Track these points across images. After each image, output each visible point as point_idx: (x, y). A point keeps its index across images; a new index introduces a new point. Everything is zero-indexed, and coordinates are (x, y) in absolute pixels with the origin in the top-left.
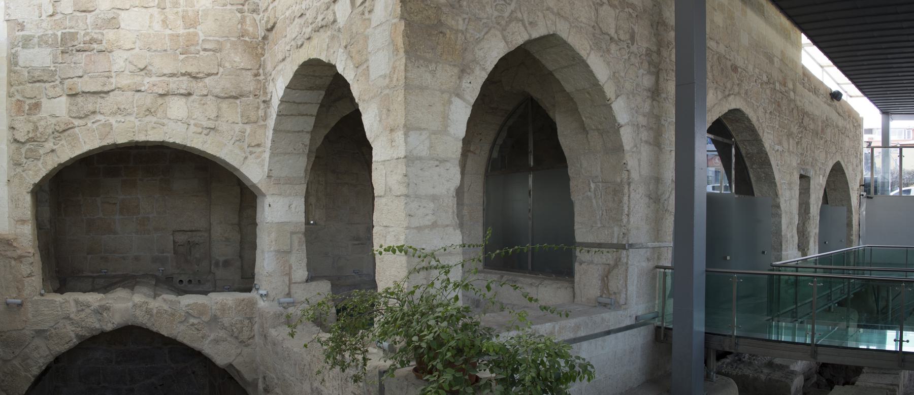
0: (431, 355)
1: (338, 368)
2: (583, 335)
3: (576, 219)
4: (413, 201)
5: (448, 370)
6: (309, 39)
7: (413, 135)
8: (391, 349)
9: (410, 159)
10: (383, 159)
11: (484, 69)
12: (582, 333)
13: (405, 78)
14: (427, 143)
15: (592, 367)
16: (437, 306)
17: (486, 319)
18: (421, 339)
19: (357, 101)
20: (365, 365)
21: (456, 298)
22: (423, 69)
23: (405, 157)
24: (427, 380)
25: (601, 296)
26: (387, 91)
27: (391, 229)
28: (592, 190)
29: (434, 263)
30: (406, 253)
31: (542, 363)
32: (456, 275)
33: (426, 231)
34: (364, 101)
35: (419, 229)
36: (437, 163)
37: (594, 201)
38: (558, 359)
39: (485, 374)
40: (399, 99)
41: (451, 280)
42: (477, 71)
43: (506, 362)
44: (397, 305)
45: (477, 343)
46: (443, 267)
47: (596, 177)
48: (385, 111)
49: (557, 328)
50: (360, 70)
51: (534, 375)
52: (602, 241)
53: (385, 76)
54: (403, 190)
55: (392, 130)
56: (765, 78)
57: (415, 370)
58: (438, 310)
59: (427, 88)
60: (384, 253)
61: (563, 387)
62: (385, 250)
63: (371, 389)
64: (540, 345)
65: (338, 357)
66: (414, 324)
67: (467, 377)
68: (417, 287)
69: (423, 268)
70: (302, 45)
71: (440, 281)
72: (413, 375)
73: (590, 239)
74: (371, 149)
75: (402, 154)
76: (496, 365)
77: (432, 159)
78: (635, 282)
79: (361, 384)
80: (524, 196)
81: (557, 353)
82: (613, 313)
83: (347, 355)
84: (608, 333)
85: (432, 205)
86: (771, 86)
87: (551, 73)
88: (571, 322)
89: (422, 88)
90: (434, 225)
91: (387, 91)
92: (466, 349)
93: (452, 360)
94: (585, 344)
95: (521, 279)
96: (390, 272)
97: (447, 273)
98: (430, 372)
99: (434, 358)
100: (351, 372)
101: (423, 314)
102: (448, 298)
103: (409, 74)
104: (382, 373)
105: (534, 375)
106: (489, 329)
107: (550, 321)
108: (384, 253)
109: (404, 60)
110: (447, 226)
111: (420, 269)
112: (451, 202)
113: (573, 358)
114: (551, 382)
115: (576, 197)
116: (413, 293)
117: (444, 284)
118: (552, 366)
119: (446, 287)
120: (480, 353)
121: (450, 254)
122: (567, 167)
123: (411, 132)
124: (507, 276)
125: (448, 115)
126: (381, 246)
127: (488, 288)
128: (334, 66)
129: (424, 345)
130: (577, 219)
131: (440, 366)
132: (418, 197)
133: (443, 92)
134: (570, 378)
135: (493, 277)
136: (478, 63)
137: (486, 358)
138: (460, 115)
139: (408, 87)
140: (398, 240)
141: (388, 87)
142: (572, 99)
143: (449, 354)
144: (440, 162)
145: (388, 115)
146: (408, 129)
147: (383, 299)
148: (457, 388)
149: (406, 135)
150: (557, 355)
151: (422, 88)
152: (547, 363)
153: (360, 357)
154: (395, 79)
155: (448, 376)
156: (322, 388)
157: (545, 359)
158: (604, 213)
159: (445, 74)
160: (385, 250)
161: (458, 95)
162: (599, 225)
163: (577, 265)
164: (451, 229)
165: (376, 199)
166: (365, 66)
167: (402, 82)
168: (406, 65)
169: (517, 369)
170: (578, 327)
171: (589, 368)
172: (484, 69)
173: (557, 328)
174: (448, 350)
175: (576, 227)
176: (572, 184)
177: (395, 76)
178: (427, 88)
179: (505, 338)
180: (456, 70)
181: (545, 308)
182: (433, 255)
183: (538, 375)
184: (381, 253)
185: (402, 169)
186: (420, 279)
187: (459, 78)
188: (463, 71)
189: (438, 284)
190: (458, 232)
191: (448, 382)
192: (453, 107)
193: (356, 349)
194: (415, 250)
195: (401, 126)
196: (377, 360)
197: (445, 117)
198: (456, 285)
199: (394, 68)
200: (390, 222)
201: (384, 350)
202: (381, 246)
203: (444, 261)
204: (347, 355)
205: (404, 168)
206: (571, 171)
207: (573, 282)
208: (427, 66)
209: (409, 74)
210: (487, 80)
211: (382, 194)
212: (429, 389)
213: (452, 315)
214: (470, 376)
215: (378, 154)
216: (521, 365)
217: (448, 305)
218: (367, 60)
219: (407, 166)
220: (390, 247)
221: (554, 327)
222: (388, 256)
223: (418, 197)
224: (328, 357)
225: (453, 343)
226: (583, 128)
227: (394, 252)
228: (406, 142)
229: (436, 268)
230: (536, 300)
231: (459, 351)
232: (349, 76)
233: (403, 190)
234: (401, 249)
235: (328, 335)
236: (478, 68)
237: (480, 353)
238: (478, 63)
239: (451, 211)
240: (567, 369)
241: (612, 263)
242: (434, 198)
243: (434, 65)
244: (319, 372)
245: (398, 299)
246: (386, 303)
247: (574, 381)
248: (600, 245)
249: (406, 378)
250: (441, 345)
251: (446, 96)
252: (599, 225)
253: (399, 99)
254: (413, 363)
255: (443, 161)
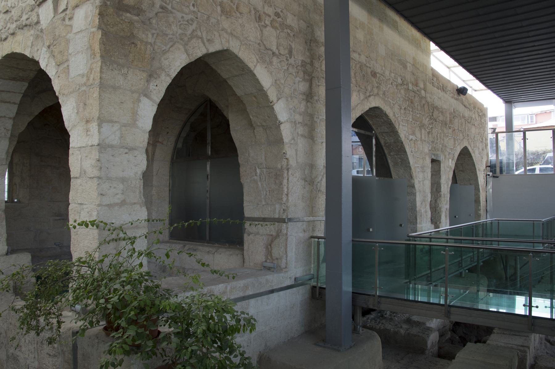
0: (117, 314)
1: (33, 333)
2: (251, 293)
3: (245, 198)
4: (105, 183)
5: (132, 327)
6: (13, 34)
7: (106, 127)
8: (84, 310)
9: (102, 147)
10: (79, 145)
11: (169, 75)
12: (250, 292)
13: (101, 78)
14: (118, 133)
15: (255, 320)
16: (123, 273)
17: (165, 283)
18: (107, 301)
19: (57, 94)
20: (59, 327)
21: (141, 265)
22: (116, 72)
23: (98, 145)
24: (113, 337)
25: (266, 261)
26: (84, 88)
27: (85, 206)
28: (258, 174)
29: (122, 235)
30: (97, 227)
31: (212, 318)
32: (141, 245)
33: (116, 208)
34: (64, 94)
35: (110, 206)
36: (126, 151)
37: (259, 183)
38: (225, 314)
39: (165, 329)
40: (95, 95)
41: (137, 250)
42: (163, 77)
43: (183, 317)
44: (89, 272)
45: (157, 302)
46: (130, 239)
47: (261, 164)
48: (82, 105)
49: (229, 288)
50: (61, 68)
51: (204, 328)
52: (266, 216)
53: (83, 76)
54: (96, 173)
55: (87, 122)
56: (399, 81)
57: (105, 329)
58: (123, 275)
59: (119, 88)
60: (78, 227)
61: (229, 338)
62: (79, 224)
63: (65, 349)
64: (209, 303)
65: (34, 323)
66: (103, 288)
67: (148, 332)
68: (106, 256)
69: (113, 239)
70: (6, 39)
71: (126, 251)
72: (103, 333)
73: (256, 214)
74: (70, 136)
75: (96, 142)
76: (174, 320)
77: (122, 147)
78: (294, 250)
79: (56, 345)
80: (204, 181)
81: (224, 309)
82: (275, 275)
83: (42, 319)
84: (272, 291)
85: (121, 186)
86: (405, 86)
87: (225, 81)
88: (241, 283)
89: (115, 88)
90: (123, 203)
91: (84, 88)
92: (148, 308)
93: (135, 318)
94: (252, 301)
95: (200, 248)
96: (84, 244)
97: (132, 243)
98: (117, 329)
99: (120, 318)
100: (46, 335)
101: (111, 280)
102: (133, 265)
103: (104, 75)
104: (75, 333)
105: (204, 328)
106: (168, 290)
107: (223, 282)
108: (78, 227)
109: (100, 63)
110: (135, 203)
111: (110, 241)
112: (138, 184)
113: (239, 314)
114: (220, 334)
115: (245, 181)
116: (102, 261)
117: (130, 254)
118: (220, 320)
119: (131, 255)
120: (161, 312)
121: (137, 227)
122: (237, 156)
123: (104, 124)
124: (189, 245)
125: (137, 111)
126: (75, 221)
127: (167, 255)
128: (38, 63)
129: (110, 306)
130: (246, 198)
131: (123, 324)
132: (109, 179)
133: (133, 92)
134: (235, 330)
135: (177, 246)
136: (163, 70)
137: (165, 314)
138: (147, 111)
139: (103, 86)
140: (91, 215)
141: (85, 84)
142: (242, 101)
143: (132, 313)
144: (130, 150)
145: (84, 109)
146: (101, 121)
147: (75, 268)
148: (139, 342)
149: (100, 126)
150: (224, 311)
151: (115, 88)
152: (216, 318)
153: (55, 321)
154: (91, 79)
155: (131, 332)
156: (19, 353)
157: (214, 314)
158: (268, 193)
159: (136, 78)
160: (79, 224)
161: (146, 95)
162: (264, 203)
163: (245, 236)
164: (138, 206)
165: (72, 181)
166: (65, 65)
167: (98, 81)
168: (101, 68)
169: (191, 324)
170: (246, 287)
171: (252, 321)
172: (169, 75)
173: (229, 288)
174: (131, 310)
175: (245, 205)
176: (242, 169)
177: (92, 76)
178: (119, 88)
179: (182, 298)
180: (145, 75)
181: (215, 271)
182: (121, 228)
183: (208, 328)
184: (75, 227)
185: (95, 154)
186: (111, 249)
187: (147, 81)
188: (151, 76)
189: (125, 254)
190: (144, 209)
191: (131, 338)
192: (141, 105)
193: (50, 313)
194: (106, 224)
195: (96, 118)
196: (71, 321)
197: (134, 114)
198: (140, 254)
199: (91, 69)
200: (85, 199)
201: (78, 313)
202: (75, 221)
203: (130, 234)
204: (42, 319)
205: (98, 154)
206: (241, 160)
207: (243, 250)
208: (120, 70)
209: (104, 75)
210: (170, 85)
211: (78, 176)
212: (114, 345)
213: (135, 280)
214: (151, 332)
215: (75, 141)
216: (194, 320)
217: (131, 271)
218: (67, 60)
219: (100, 152)
220: (83, 222)
221: (226, 287)
222: (82, 230)
223: (109, 179)
224: (23, 323)
225: (135, 303)
226: (251, 125)
227: (87, 226)
228: (99, 132)
229: (124, 239)
230: (208, 265)
231: (142, 310)
232: (51, 72)
233: (96, 173)
234: (93, 223)
235: (23, 303)
236: (163, 74)
237: (161, 312)
238: (163, 70)
239: (138, 191)
240: (234, 323)
241: (274, 234)
242: (123, 180)
243: (126, 70)
244: (14, 338)
245: (89, 267)
246: (78, 271)
247: (239, 332)
248: (264, 220)
249: (97, 336)
250: (126, 306)
251: (136, 96)
252: (264, 203)
253: (95, 95)
254: (103, 323)
255: (132, 149)
